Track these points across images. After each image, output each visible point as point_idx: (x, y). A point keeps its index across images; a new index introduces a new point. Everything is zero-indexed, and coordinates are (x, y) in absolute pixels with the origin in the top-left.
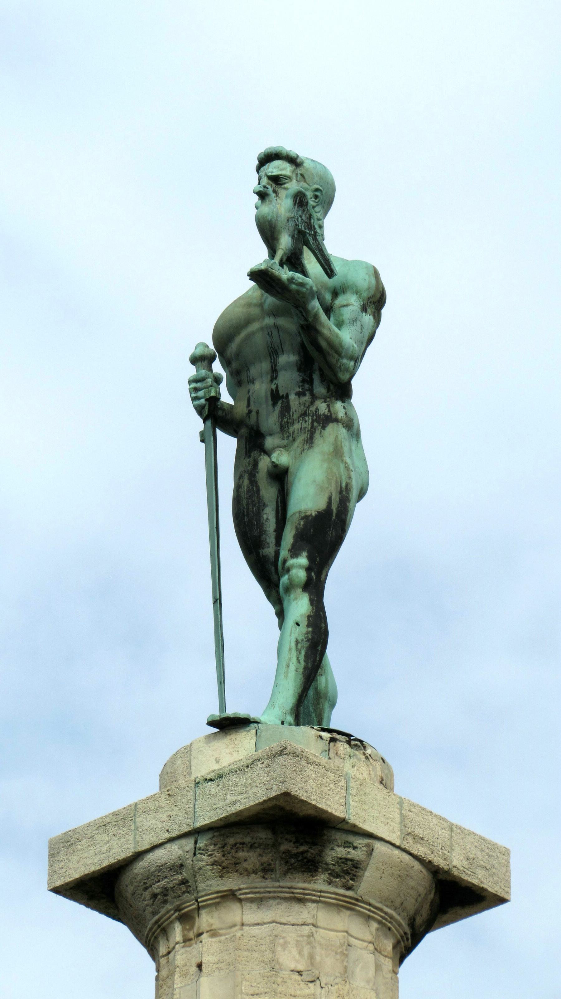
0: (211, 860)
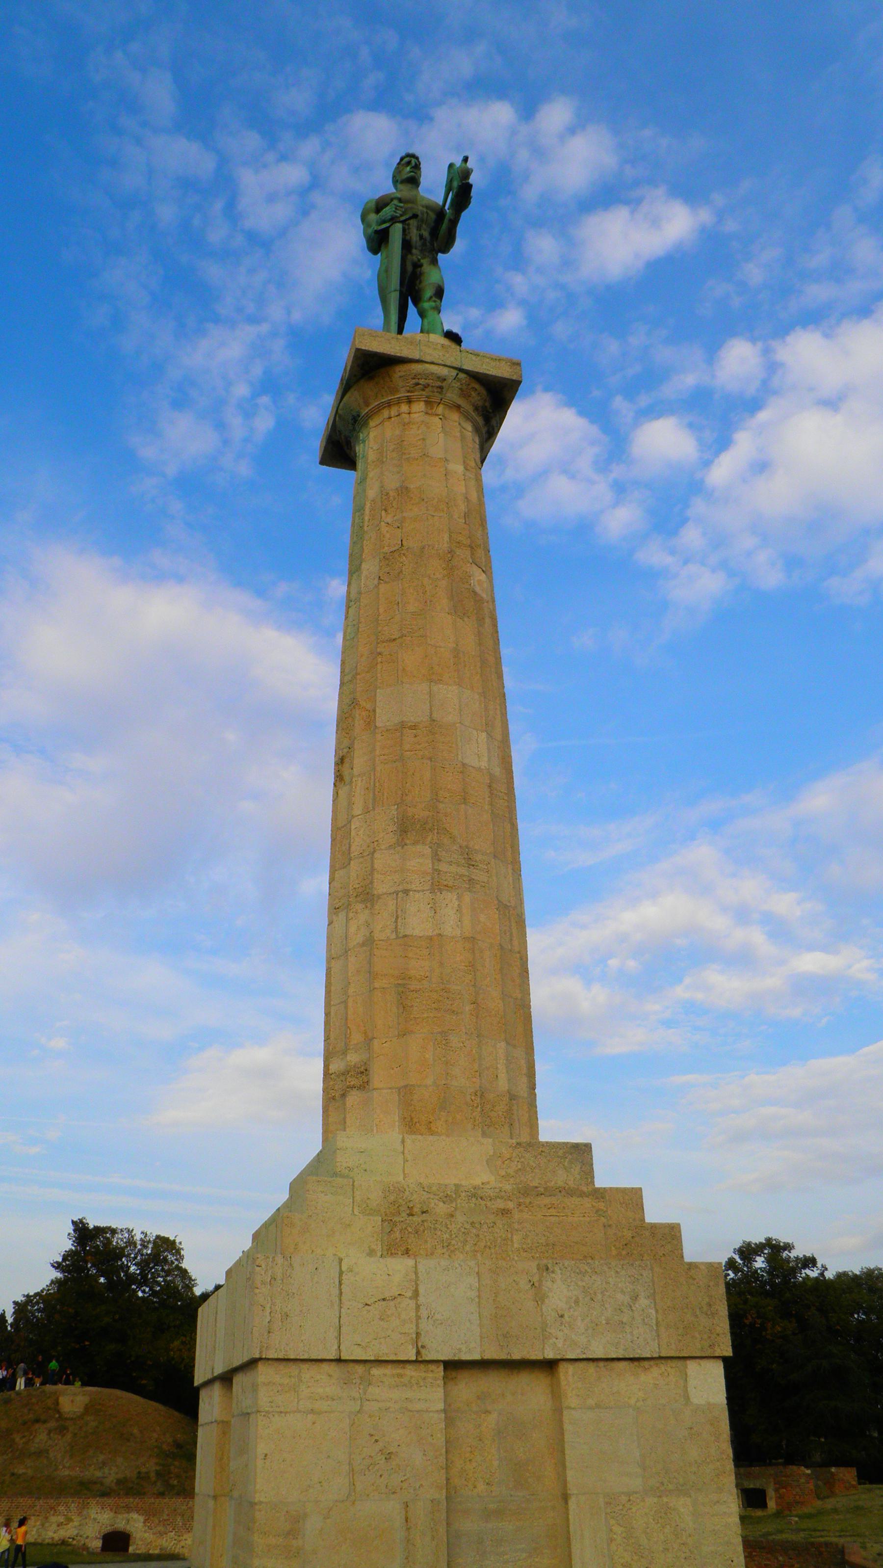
0: (460, 387)
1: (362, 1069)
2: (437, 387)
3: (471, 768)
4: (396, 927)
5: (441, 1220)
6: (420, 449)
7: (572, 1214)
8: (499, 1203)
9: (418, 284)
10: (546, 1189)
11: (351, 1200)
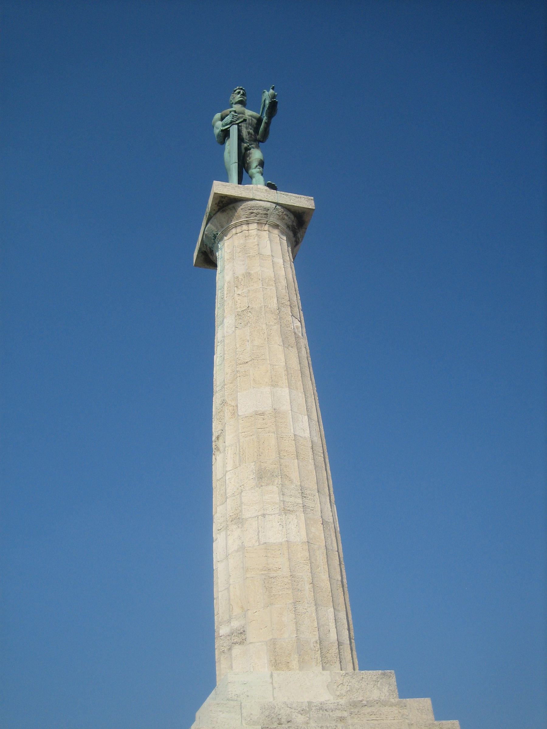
1: (241, 631)
2: (264, 214)
3: (299, 437)
4: (258, 538)
5: (301, 726)
6: (255, 250)
7: (386, 718)
8: (338, 714)
9: (248, 160)
10: (367, 702)
11: (240, 716)
